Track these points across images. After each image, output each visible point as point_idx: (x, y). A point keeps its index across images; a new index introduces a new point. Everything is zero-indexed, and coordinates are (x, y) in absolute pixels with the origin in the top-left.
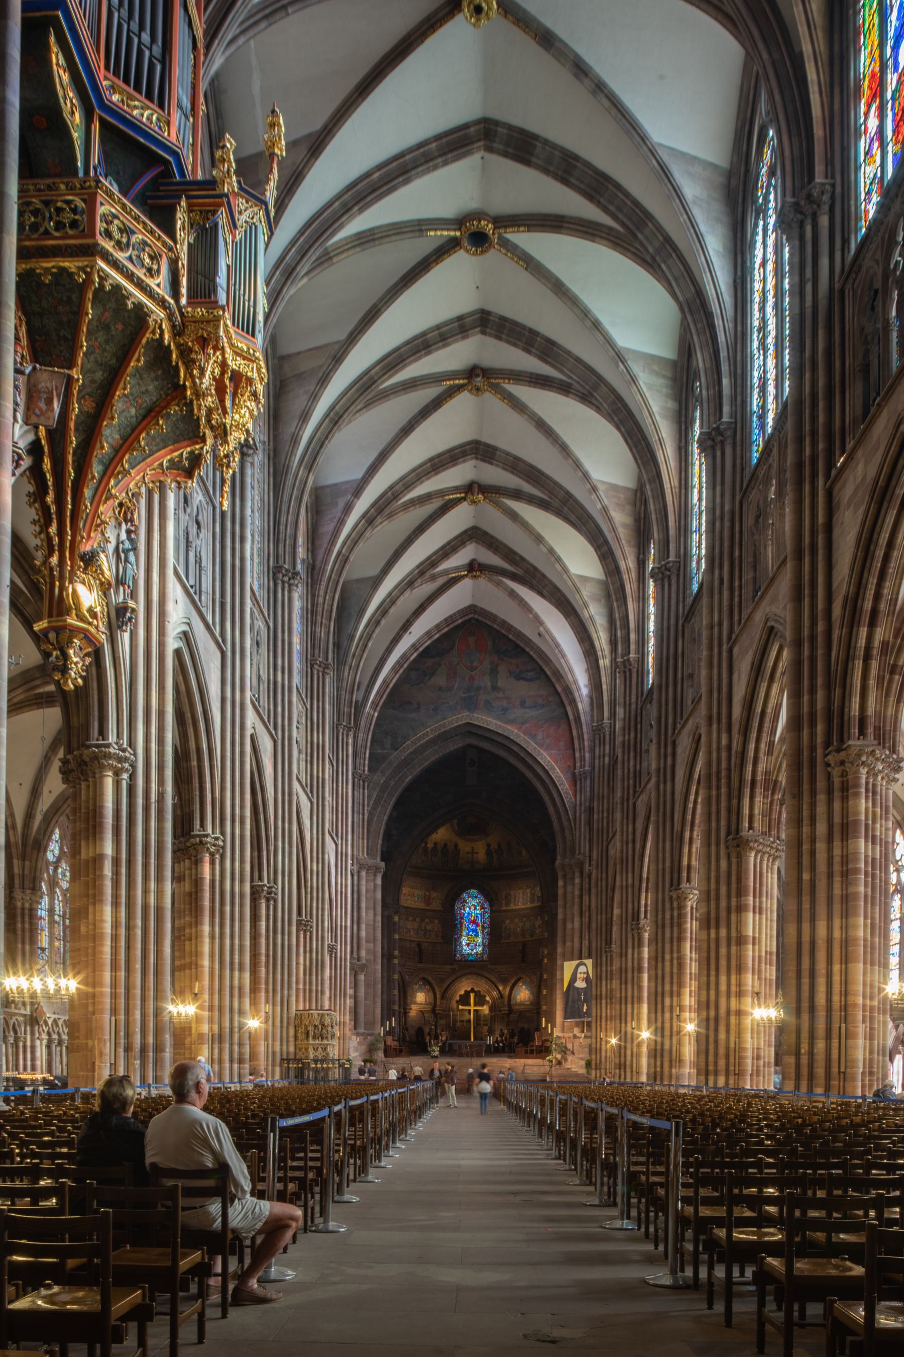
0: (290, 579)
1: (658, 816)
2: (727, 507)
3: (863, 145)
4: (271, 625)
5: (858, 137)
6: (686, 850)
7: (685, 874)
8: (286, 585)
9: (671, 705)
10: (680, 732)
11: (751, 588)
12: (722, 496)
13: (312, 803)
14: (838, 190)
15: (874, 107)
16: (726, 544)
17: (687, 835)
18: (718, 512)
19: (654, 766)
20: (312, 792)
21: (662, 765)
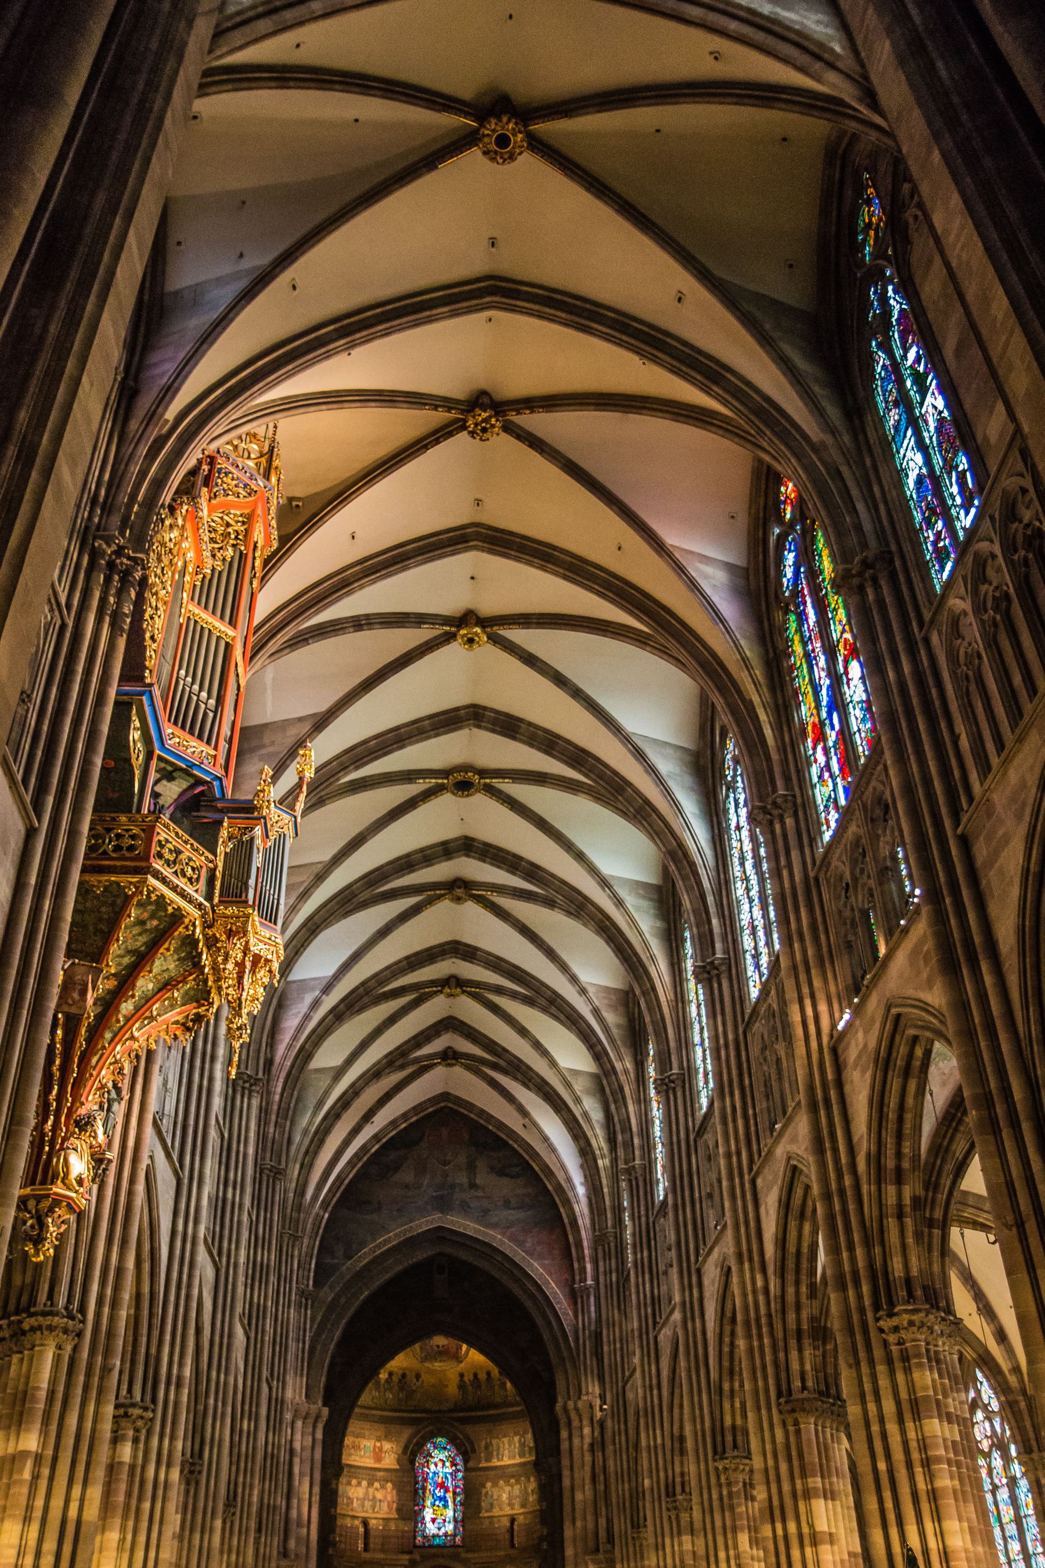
0: (251, 1085)
1: (688, 1361)
2: (731, 1037)
3: (814, 770)
4: (226, 1135)
5: (809, 765)
6: (727, 1406)
7: (729, 1438)
8: (247, 1092)
9: (690, 1227)
10: (705, 1261)
11: (766, 1116)
12: (724, 1024)
13: (248, 1339)
14: (799, 800)
15: (819, 748)
16: (734, 1072)
17: (726, 1386)
18: (722, 1041)
19: (677, 1298)
20: (249, 1324)
21: (687, 1299)
